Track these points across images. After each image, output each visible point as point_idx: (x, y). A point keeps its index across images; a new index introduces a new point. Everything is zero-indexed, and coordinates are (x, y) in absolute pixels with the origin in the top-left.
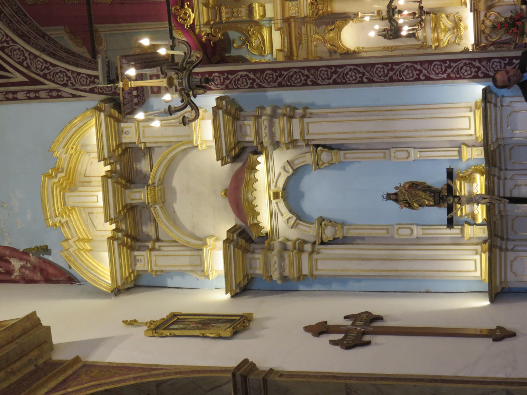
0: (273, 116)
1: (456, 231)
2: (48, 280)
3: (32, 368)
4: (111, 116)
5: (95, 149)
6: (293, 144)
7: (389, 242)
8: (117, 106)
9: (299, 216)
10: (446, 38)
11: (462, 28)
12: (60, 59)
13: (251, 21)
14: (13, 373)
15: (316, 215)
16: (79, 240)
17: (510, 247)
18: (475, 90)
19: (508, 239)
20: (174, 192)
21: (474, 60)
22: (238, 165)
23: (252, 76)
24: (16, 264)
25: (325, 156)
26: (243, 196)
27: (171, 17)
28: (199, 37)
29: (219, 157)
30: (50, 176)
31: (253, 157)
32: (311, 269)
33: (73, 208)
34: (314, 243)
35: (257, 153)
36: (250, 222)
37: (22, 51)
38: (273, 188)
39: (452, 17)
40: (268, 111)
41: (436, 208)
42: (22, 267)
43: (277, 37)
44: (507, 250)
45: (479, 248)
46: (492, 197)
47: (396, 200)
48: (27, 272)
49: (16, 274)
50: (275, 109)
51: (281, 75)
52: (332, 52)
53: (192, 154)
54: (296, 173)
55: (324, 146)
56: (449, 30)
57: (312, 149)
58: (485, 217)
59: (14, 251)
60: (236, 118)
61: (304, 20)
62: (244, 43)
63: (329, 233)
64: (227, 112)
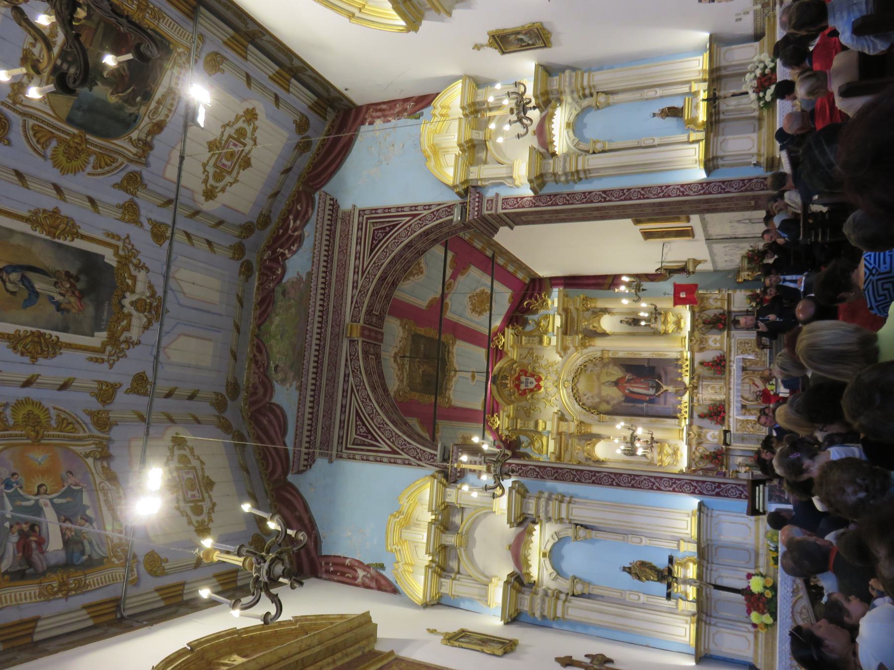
0: (549, 499)
1: (672, 603)
2: (380, 588)
3: (360, 653)
4: (441, 482)
5: (428, 503)
6: (560, 520)
7: (621, 603)
8: (446, 476)
9: (559, 572)
10: (667, 460)
12: (414, 440)
13: (536, 431)
14: (347, 655)
15: (570, 574)
16: (406, 564)
17: (713, 623)
18: (693, 502)
19: (711, 616)
20: (475, 542)
21: (693, 481)
22: (521, 529)
23: (537, 470)
24: (361, 573)
25: (582, 532)
26: (522, 551)
27: (485, 421)
28: (500, 437)
29: (509, 522)
30: (395, 516)
31: (531, 525)
32: (563, 613)
33: (406, 541)
34: (567, 594)
35: (534, 522)
36: (524, 571)
37: (391, 431)
38: (543, 549)
40: (546, 495)
41: (658, 583)
42: (364, 576)
43: (552, 444)
44: (710, 624)
45: (689, 619)
46: (701, 581)
47: (630, 573)
48: (367, 580)
49: (359, 580)
50: (550, 494)
51: (557, 472)
52: (587, 459)
53: (491, 517)
54: (560, 542)
55: (582, 525)
57: (573, 526)
58: (695, 596)
59: (361, 563)
60: (523, 497)
61: (571, 435)
62: (529, 444)
63: (579, 589)
64: (518, 492)
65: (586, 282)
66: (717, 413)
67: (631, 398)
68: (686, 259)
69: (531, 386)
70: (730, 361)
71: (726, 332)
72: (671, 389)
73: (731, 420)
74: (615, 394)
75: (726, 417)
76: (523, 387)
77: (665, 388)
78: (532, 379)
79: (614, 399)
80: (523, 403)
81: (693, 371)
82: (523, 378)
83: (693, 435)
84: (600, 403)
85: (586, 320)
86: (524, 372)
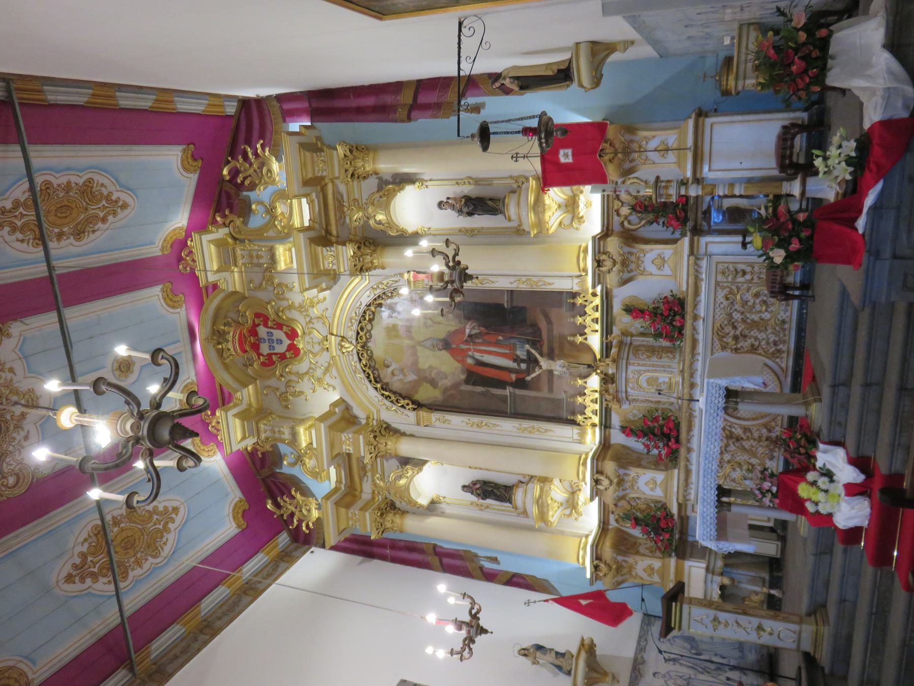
10: (554, 515)
11: (580, 503)
39: (567, 484)
56: (562, 504)
65: (354, 103)
66: (663, 435)
67: (477, 376)
68: (570, 43)
69: (281, 349)
70: (695, 318)
71: (686, 241)
72: (558, 367)
73: (694, 456)
74: (447, 367)
75: (683, 451)
76: (265, 349)
77: (545, 363)
78: (278, 334)
79: (446, 377)
80: (272, 382)
81: (607, 330)
82: (262, 331)
83: (606, 482)
84: (416, 385)
85: (360, 208)
86: (263, 318)
